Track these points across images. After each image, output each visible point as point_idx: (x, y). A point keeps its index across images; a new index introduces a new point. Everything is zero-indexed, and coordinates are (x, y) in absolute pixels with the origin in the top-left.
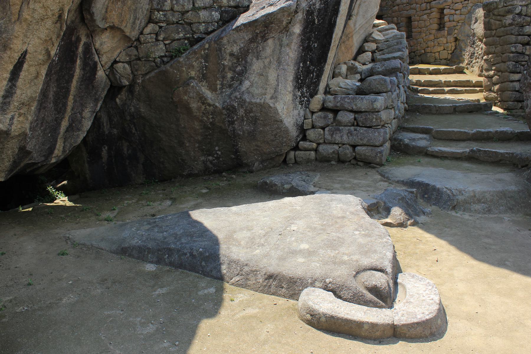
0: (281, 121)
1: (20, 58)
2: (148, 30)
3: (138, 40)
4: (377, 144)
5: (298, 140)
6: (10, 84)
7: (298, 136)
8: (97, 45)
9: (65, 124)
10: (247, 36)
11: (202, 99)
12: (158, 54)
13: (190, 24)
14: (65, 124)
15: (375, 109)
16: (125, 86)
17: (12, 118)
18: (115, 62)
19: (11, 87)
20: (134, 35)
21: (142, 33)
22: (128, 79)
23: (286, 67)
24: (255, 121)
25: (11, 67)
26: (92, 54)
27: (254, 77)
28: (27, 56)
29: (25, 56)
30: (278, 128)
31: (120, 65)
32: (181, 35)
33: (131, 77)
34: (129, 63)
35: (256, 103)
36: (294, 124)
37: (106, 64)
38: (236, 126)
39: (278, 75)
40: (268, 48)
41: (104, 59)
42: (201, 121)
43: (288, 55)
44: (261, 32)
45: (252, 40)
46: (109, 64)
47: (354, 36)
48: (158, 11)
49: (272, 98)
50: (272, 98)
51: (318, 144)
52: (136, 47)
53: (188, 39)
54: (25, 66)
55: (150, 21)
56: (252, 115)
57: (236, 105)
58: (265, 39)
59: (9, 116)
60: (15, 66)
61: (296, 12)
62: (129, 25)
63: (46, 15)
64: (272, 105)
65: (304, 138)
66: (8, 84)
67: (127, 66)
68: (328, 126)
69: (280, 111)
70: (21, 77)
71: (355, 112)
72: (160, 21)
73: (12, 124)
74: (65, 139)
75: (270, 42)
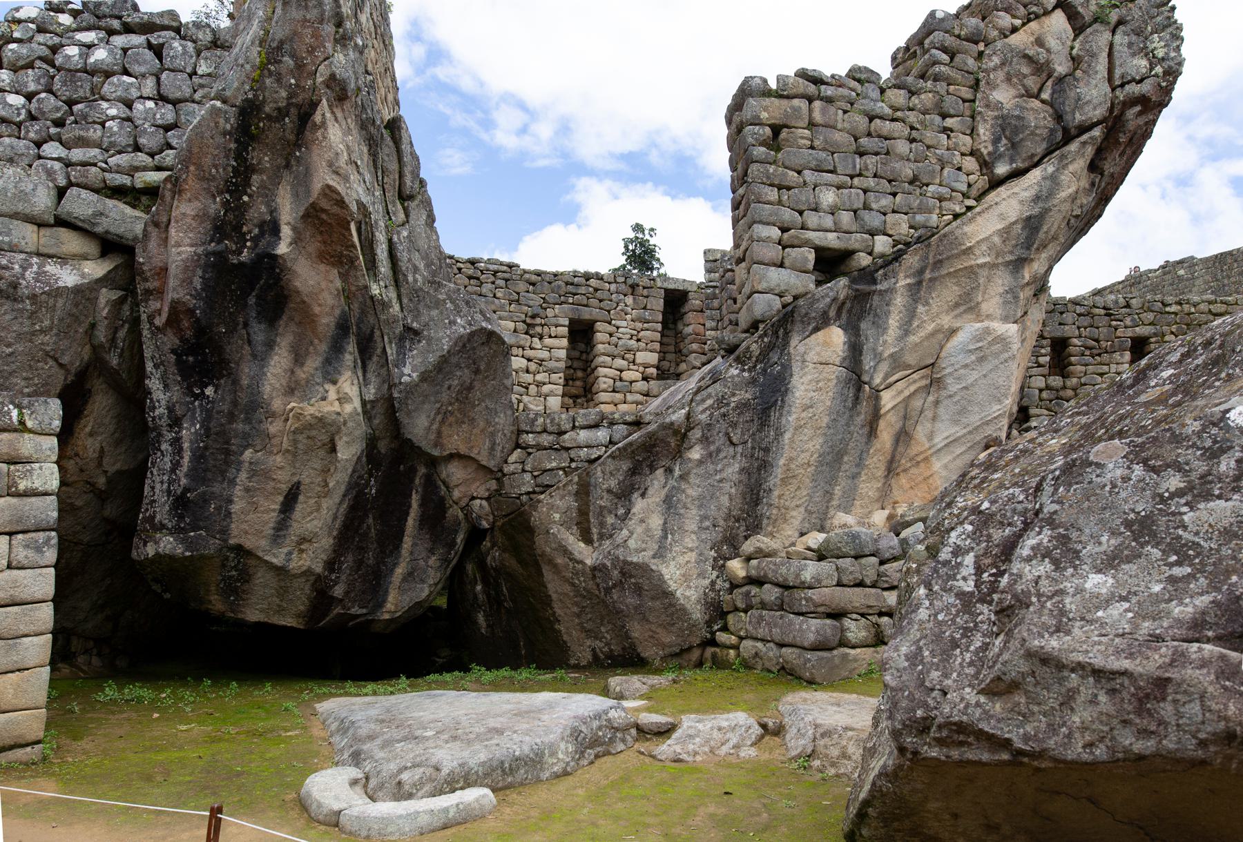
0: (672, 594)
2: (512, 458)
3: (501, 470)
4: (806, 644)
5: (716, 627)
7: (709, 623)
8: (443, 476)
10: (625, 465)
11: (566, 552)
12: (524, 489)
13: (567, 449)
15: (803, 583)
16: (487, 530)
18: (473, 498)
20: (492, 464)
21: (506, 462)
22: (487, 520)
23: (682, 511)
24: (638, 590)
26: (437, 487)
27: (632, 523)
29: (298, 488)
30: (671, 605)
31: (478, 502)
32: (554, 464)
33: (491, 518)
34: (488, 499)
35: (632, 563)
36: (699, 601)
37: (460, 499)
38: (615, 597)
39: (665, 523)
40: (656, 482)
41: (456, 494)
42: (573, 585)
43: (684, 491)
44: (644, 459)
45: (634, 471)
46: (466, 500)
47: (934, 459)
48: (527, 433)
49: (654, 557)
50: (654, 557)
51: (741, 638)
52: (497, 479)
53: (563, 469)
55: (518, 446)
56: (633, 580)
57: (609, 564)
58: (653, 469)
61: (689, 429)
62: (485, 453)
64: (654, 567)
65: (725, 629)
67: (484, 503)
68: (752, 608)
69: (667, 577)
71: (786, 587)
72: (529, 446)
75: (660, 472)
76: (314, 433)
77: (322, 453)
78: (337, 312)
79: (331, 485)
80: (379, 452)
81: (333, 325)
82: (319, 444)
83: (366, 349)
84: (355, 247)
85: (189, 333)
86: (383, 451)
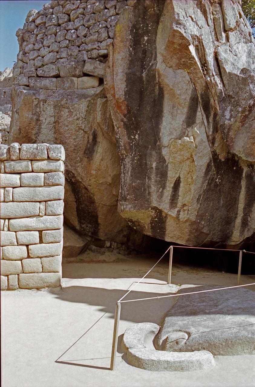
1: (176, 181)
6: (173, 193)
9: (239, 221)
14: (239, 221)
17: (179, 211)
19: (174, 195)
25: (172, 185)
28: (181, 180)
54: (181, 185)
59: (177, 210)
60: (175, 184)
63: (184, 159)
66: (172, 194)
70: (180, 190)
73: (180, 214)
74: (242, 232)
76: (182, 153)
77: (188, 162)
78: (190, 92)
79: (194, 178)
80: (220, 160)
81: (188, 99)
82: (186, 158)
83: (207, 108)
84: (194, 58)
85: (126, 112)
86: (223, 160)
